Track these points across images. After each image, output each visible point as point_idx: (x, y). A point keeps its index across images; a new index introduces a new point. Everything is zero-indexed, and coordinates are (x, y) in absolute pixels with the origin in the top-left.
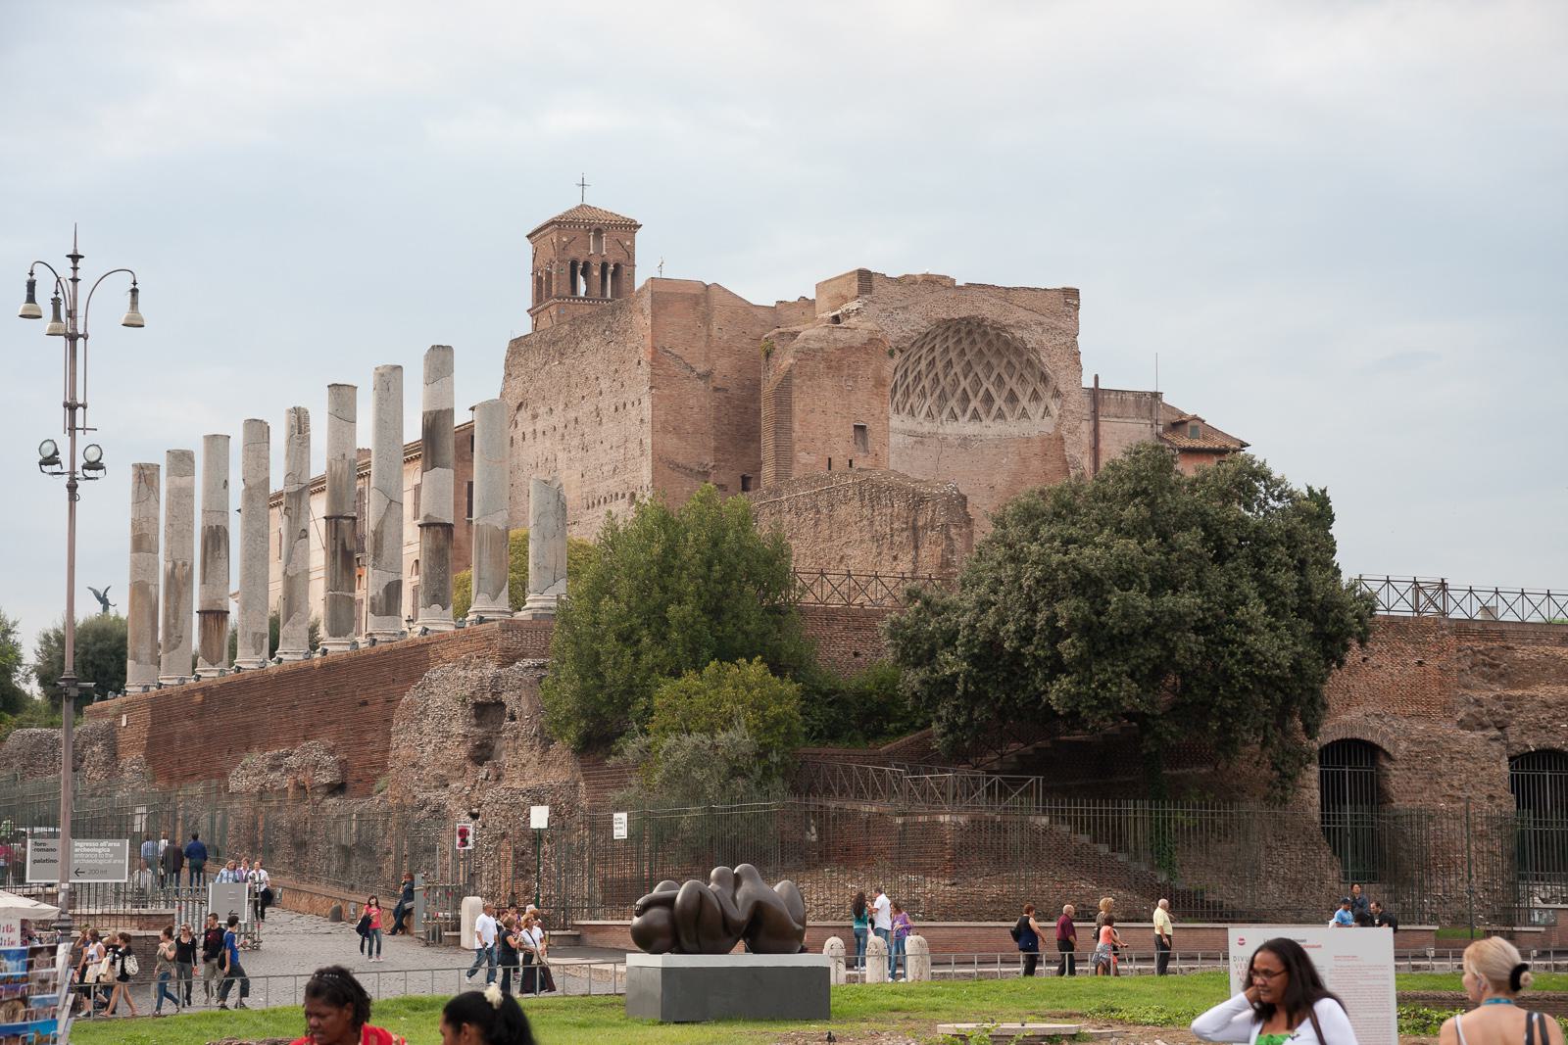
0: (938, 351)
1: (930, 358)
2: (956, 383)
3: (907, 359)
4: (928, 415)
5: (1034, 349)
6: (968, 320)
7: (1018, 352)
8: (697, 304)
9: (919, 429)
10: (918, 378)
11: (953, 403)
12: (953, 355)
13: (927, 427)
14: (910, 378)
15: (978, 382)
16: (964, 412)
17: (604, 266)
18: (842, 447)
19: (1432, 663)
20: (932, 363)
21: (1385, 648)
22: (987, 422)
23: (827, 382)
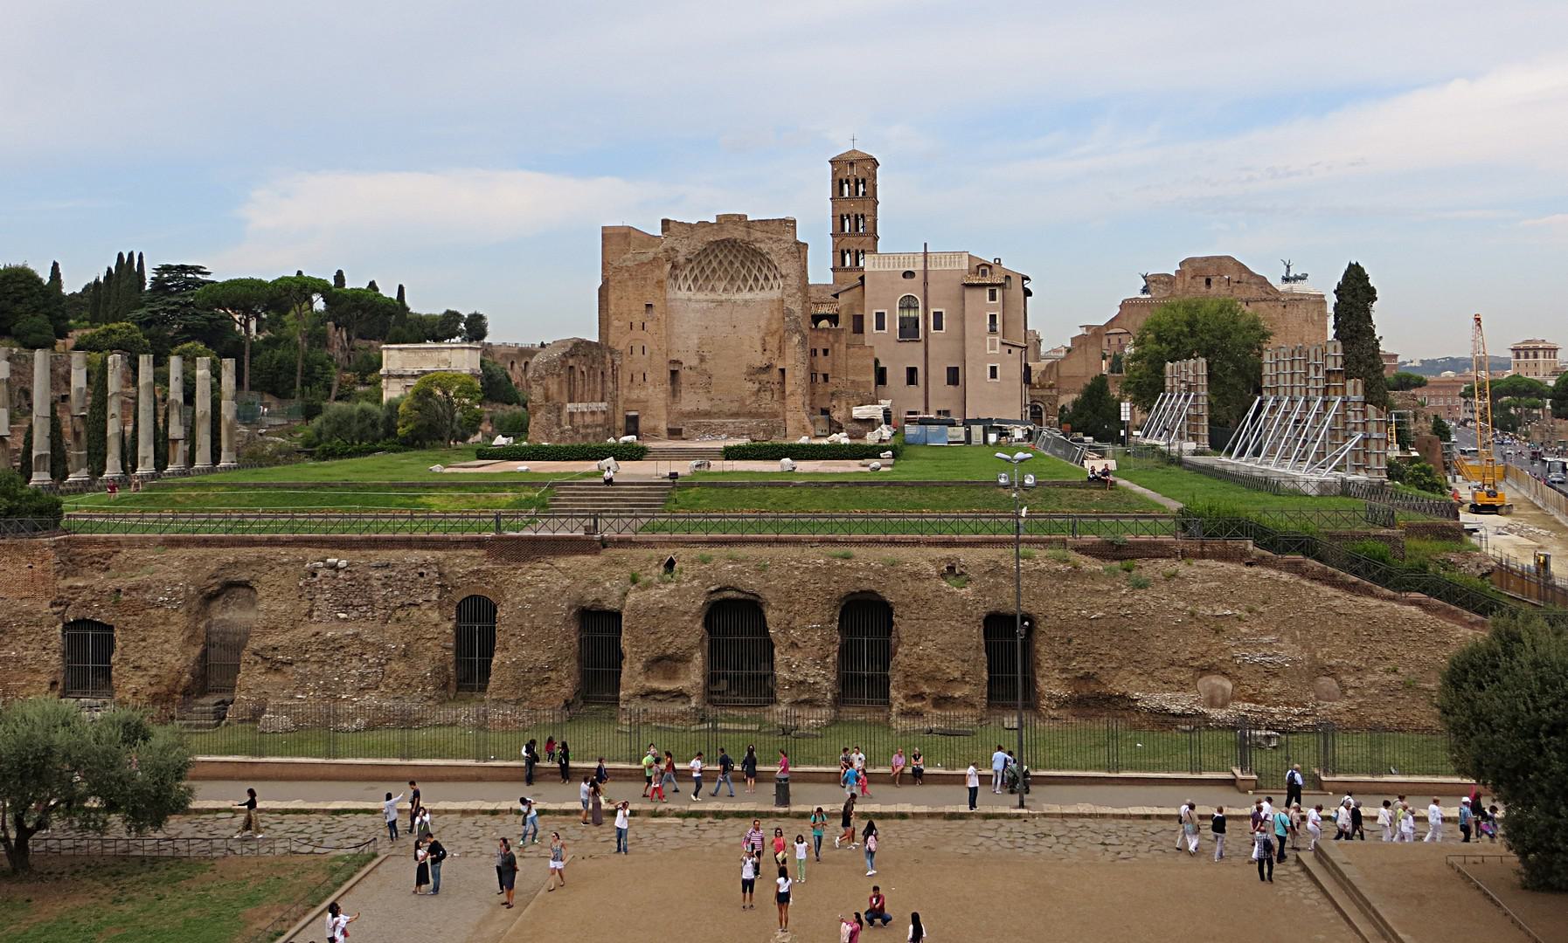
0: (721, 257)
1: (718, 260)
2: (738, 271)
3: (699, 262)
4: (725, 290)
5: (768, 253)
6: (728, 240)
7: (762, 255)
8: (626, 237)
9: (719, 298)
10: (714, 271)
11: (739, 282)
12: (731, 258)
13: (725, 296)
14: (708, 272)
15: (749, 271)
16: (745, 287)
17: (857, 181)
18: (637, 319)
19: (38, 567)
20: (720, 262)
21: (8, 558)
22: (757, 291)
23: (630, 283)
